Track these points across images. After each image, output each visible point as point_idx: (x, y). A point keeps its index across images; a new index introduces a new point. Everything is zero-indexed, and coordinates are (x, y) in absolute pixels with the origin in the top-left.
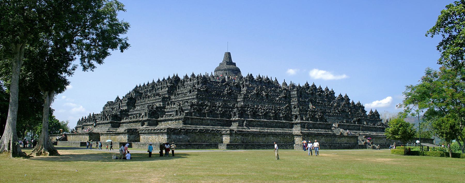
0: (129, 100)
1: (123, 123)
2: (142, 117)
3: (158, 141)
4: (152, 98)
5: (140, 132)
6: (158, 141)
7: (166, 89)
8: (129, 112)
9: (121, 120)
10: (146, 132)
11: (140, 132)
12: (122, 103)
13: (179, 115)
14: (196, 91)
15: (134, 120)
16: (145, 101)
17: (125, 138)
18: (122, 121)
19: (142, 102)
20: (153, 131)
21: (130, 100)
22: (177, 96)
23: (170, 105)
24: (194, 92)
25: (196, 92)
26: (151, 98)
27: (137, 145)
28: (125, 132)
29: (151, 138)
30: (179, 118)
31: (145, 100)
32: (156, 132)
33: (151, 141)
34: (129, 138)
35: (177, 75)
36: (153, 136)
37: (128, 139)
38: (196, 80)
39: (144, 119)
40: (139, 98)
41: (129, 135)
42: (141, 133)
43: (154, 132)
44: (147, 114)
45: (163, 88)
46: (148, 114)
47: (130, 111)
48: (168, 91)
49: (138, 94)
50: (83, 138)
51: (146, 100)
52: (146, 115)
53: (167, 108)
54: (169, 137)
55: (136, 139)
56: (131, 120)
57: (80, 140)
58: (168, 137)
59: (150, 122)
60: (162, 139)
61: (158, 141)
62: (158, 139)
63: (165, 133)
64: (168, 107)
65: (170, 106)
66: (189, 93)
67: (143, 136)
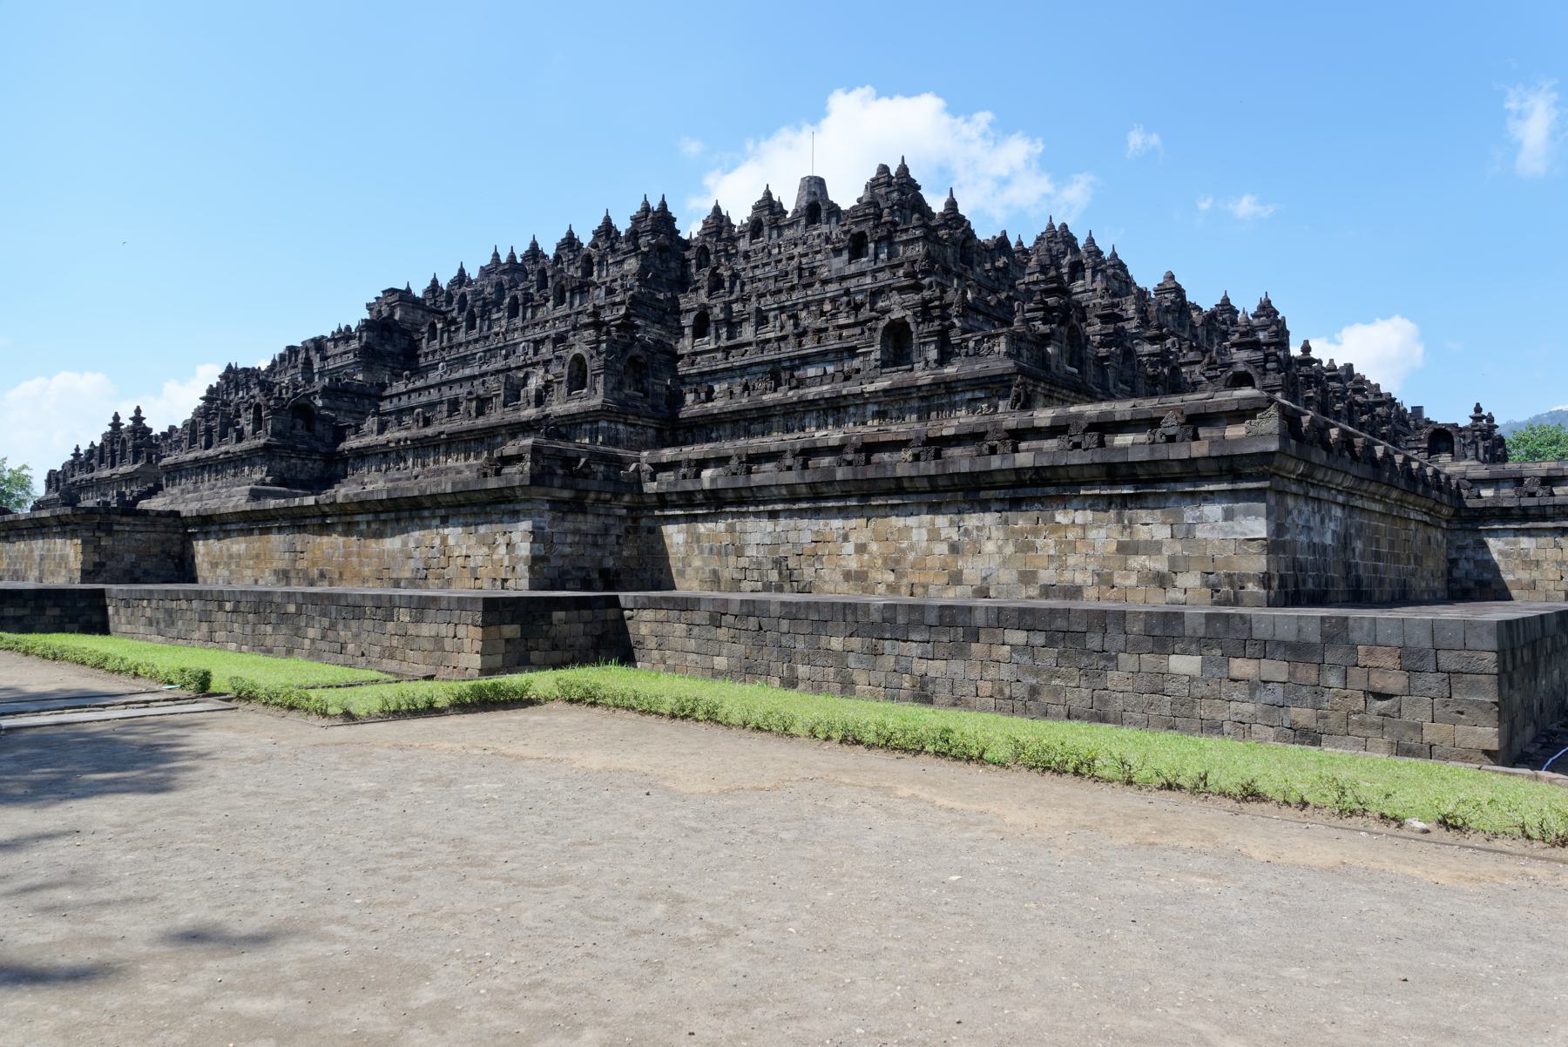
0: (371, 334)
1: (362, 455)
2: (540, 400)
3: (1027, 577)
4: (539, 314)
5: (650, 487)
6: (1008, 576)
7: (626, 267)
8: (383, 399)
9: (343, 439)
10: (765, 474)
11: (650, 487)
12: (329, 354)
13: (932, 353)
14: (916, 239)
15: (461, 423)
16: (485, 333)
17: (493, 545)
18: (352, 443)
19: (460, 345)
20: (907, 454)
21: (382, 338)
22: (731, 292)
23: (724, 332)
24: (891, 244)
25: (906, 243)
26: (529, 315)
27: (722, 633)
28: (493, 483)
29: (861, 548)
30: (936, 384)
31: (485, 328)
32: (996, 462)
33: (856, 577)
34: (541, 550)
35: (664, 205)
36: (897, 522)
37: (535, 561)
38: (803, 222)
39: (558, 407)
40: (439, 326)
41: (548, 517)
42: (663, 500)
43: (930, 467)
44: (593, 365)
45: (600, 263)
46: (607, 367)
47: (388, 392)
48: (641, 275)
49: (421, 312)
50: (37, 554)
51: (490, 328)
52: (578, 378)
53: (696, 354)
54: (1279, 529)
55: (610, 563)
56: (429, 431)
57: (16, 572)
58: (1273, 526)
59: (621, 427)
60: (1125, 549)
61: (1027, 577)
62: (1028, 547)
63: (1230, 467)
64: (708, 343)
65: (718, 337)
66: (845, 256)
67: (702, 528)
